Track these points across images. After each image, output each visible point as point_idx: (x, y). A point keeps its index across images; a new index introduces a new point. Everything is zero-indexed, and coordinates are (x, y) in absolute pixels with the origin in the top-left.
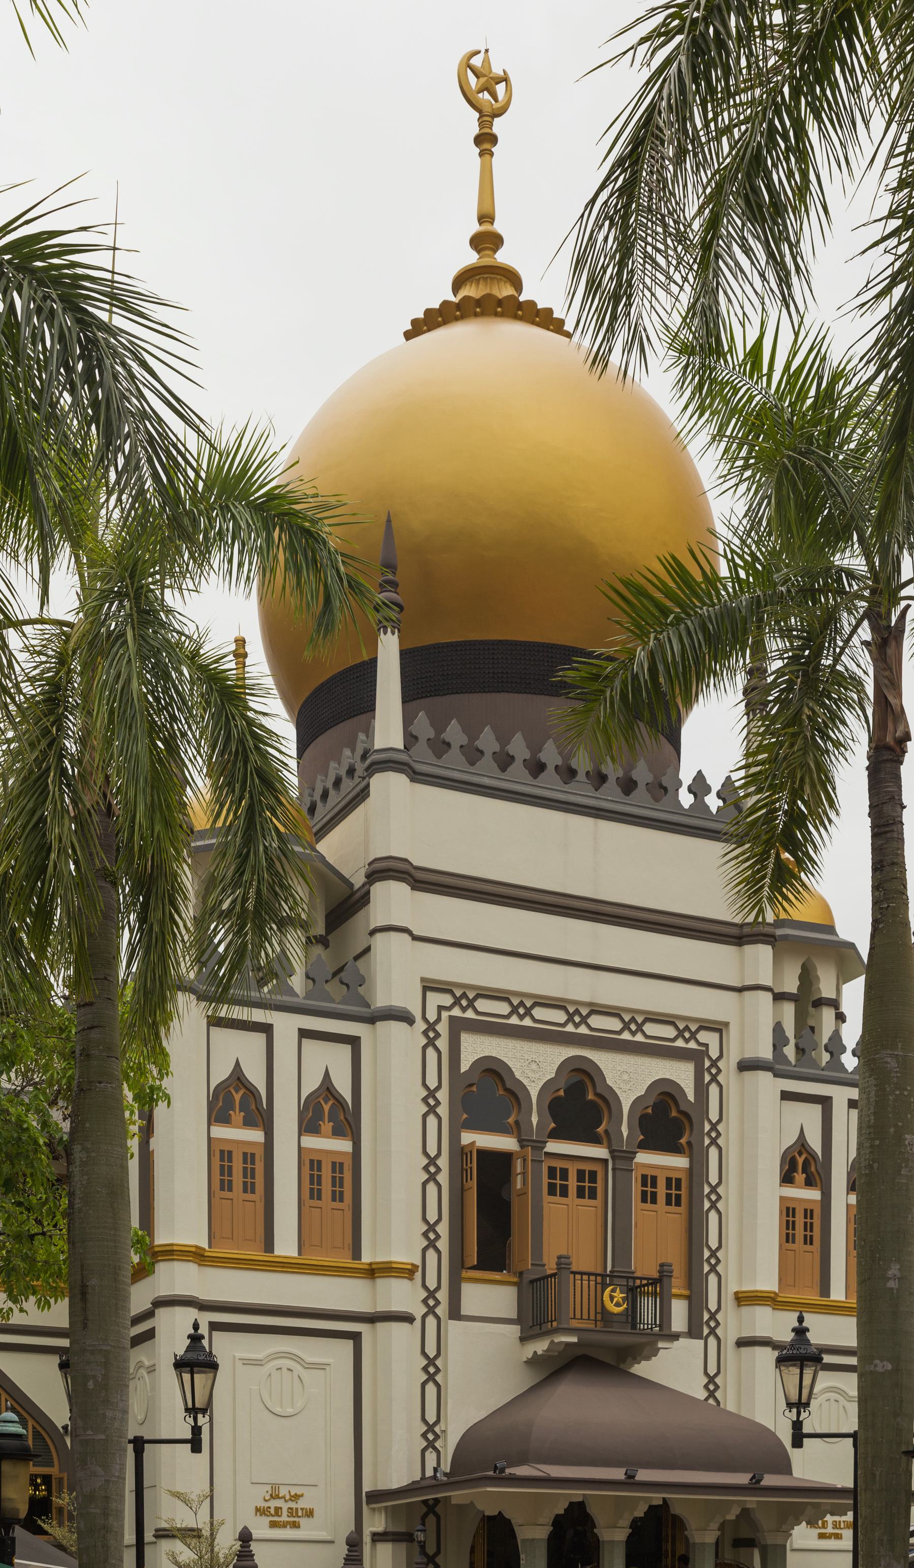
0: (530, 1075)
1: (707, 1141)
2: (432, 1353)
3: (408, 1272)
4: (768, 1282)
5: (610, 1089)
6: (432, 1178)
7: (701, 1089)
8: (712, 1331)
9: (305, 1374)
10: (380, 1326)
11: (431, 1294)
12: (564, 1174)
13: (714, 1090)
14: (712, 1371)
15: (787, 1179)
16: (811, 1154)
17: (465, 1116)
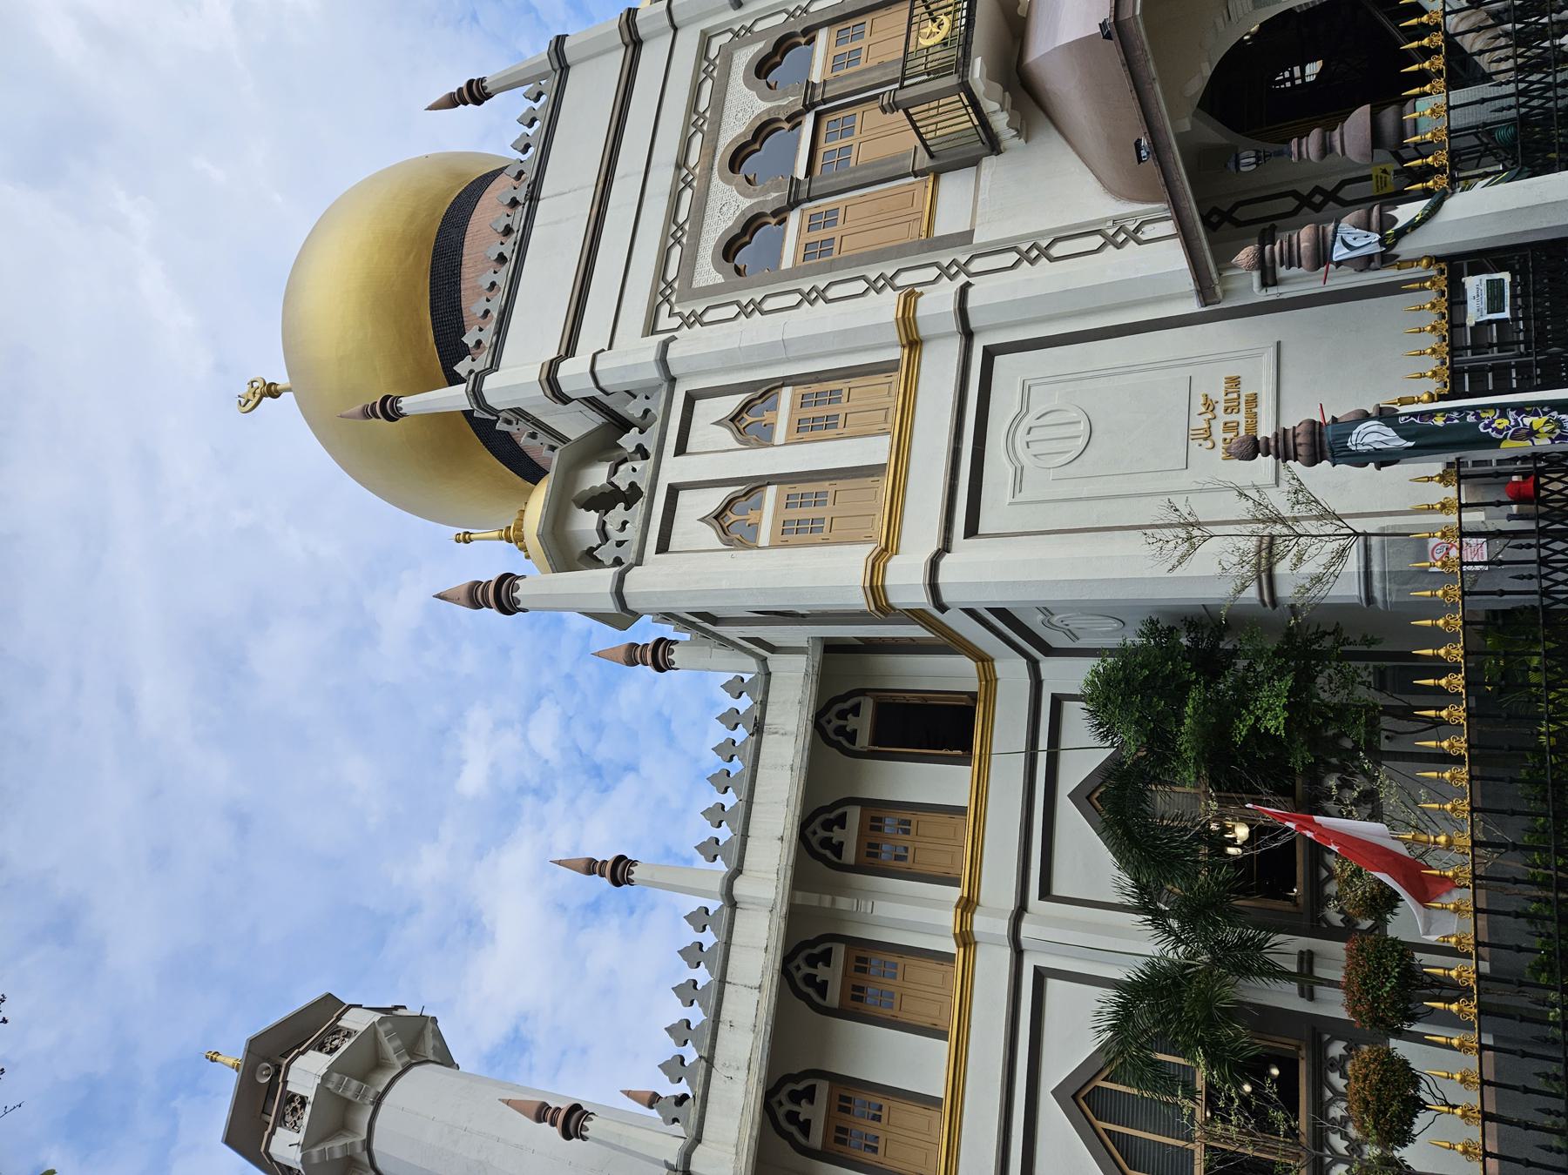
0: (732, 211)
2: (1015, 256)
9: (1034, 413)
10: (973, 324)
11: (944, 271)
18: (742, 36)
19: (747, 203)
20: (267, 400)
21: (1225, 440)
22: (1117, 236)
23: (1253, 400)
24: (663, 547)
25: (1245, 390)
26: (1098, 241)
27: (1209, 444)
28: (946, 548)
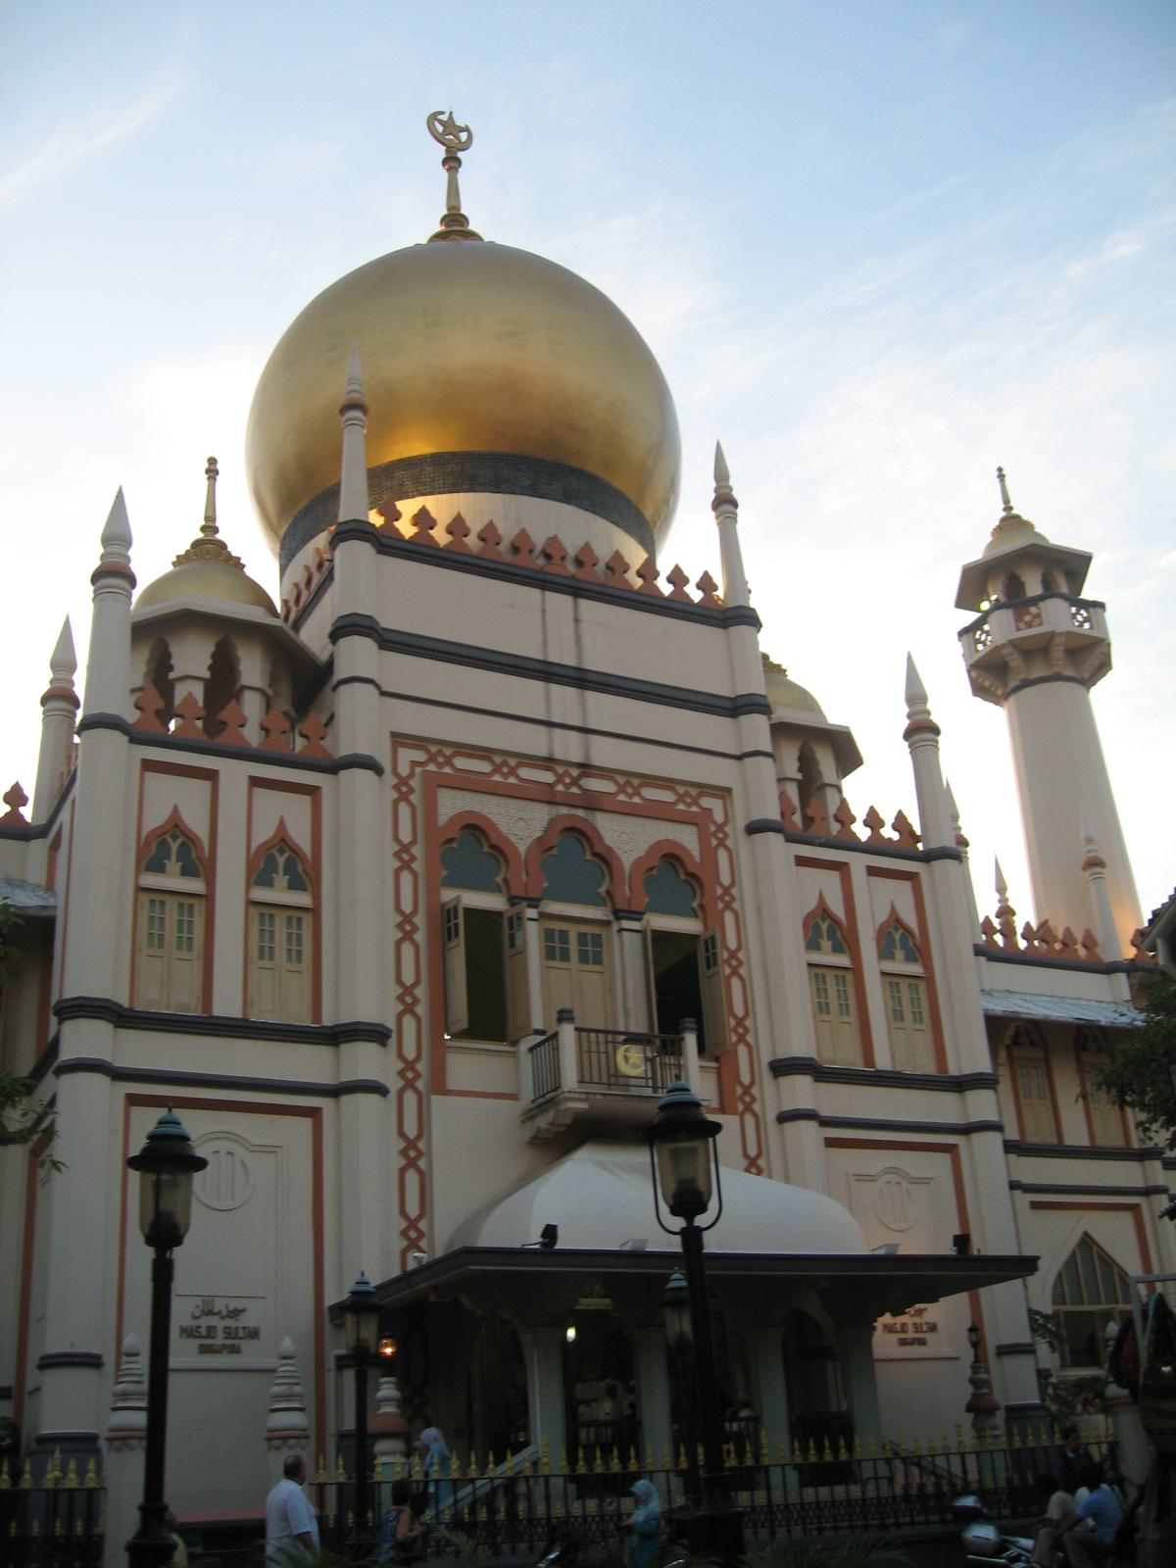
1: (721, 906)
3: (377, 1034)
4: (801, 1046)
5: (610, 849)
6: (408, 936)
7: (708, 853)
8: (748, 1108)
10: (346, 1100)
11: (410, 1065)
12: (564, 935)
13: (722, 855)
14: (752, 1151)
15: (812, 944)
16: (834, 920)
17: (444, 873)
18: (713, 835)
19: (522, 848)
20: (441, 152)
21: (199, 1327)
22: (413, 1233)
23: (234, 1350)
24: (148, 766)
25: (247, 1345)
26: (413, 1210)
27: (197, 1315)
28: (118, 1075)
